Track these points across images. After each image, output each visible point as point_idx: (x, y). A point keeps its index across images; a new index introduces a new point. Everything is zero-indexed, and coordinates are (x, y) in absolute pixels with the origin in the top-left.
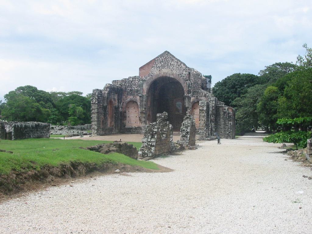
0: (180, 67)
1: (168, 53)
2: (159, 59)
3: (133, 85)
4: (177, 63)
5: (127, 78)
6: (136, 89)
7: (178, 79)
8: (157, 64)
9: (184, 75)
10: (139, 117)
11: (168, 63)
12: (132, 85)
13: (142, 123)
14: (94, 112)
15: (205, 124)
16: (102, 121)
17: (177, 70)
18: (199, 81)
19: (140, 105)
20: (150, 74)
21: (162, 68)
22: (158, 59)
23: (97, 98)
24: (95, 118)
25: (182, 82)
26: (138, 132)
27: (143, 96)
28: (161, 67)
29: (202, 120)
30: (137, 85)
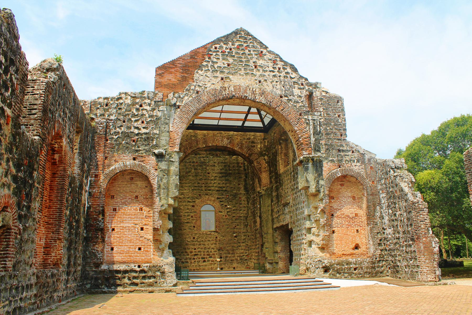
0: (283, 74)
1: (248, 34)
2: (221, 47)
4: (275, 62)
6: (143, 131)
8: (215, 60)
9: (296, 98)
11: (248, 61)
17: (274, 83)
18: (339, 116)
19: (159, 186)
20: (193, 87)
21: (229, 73)
22: (218, 46)
25: (292, 117)
28: (226, 71)
30: (149, 119)
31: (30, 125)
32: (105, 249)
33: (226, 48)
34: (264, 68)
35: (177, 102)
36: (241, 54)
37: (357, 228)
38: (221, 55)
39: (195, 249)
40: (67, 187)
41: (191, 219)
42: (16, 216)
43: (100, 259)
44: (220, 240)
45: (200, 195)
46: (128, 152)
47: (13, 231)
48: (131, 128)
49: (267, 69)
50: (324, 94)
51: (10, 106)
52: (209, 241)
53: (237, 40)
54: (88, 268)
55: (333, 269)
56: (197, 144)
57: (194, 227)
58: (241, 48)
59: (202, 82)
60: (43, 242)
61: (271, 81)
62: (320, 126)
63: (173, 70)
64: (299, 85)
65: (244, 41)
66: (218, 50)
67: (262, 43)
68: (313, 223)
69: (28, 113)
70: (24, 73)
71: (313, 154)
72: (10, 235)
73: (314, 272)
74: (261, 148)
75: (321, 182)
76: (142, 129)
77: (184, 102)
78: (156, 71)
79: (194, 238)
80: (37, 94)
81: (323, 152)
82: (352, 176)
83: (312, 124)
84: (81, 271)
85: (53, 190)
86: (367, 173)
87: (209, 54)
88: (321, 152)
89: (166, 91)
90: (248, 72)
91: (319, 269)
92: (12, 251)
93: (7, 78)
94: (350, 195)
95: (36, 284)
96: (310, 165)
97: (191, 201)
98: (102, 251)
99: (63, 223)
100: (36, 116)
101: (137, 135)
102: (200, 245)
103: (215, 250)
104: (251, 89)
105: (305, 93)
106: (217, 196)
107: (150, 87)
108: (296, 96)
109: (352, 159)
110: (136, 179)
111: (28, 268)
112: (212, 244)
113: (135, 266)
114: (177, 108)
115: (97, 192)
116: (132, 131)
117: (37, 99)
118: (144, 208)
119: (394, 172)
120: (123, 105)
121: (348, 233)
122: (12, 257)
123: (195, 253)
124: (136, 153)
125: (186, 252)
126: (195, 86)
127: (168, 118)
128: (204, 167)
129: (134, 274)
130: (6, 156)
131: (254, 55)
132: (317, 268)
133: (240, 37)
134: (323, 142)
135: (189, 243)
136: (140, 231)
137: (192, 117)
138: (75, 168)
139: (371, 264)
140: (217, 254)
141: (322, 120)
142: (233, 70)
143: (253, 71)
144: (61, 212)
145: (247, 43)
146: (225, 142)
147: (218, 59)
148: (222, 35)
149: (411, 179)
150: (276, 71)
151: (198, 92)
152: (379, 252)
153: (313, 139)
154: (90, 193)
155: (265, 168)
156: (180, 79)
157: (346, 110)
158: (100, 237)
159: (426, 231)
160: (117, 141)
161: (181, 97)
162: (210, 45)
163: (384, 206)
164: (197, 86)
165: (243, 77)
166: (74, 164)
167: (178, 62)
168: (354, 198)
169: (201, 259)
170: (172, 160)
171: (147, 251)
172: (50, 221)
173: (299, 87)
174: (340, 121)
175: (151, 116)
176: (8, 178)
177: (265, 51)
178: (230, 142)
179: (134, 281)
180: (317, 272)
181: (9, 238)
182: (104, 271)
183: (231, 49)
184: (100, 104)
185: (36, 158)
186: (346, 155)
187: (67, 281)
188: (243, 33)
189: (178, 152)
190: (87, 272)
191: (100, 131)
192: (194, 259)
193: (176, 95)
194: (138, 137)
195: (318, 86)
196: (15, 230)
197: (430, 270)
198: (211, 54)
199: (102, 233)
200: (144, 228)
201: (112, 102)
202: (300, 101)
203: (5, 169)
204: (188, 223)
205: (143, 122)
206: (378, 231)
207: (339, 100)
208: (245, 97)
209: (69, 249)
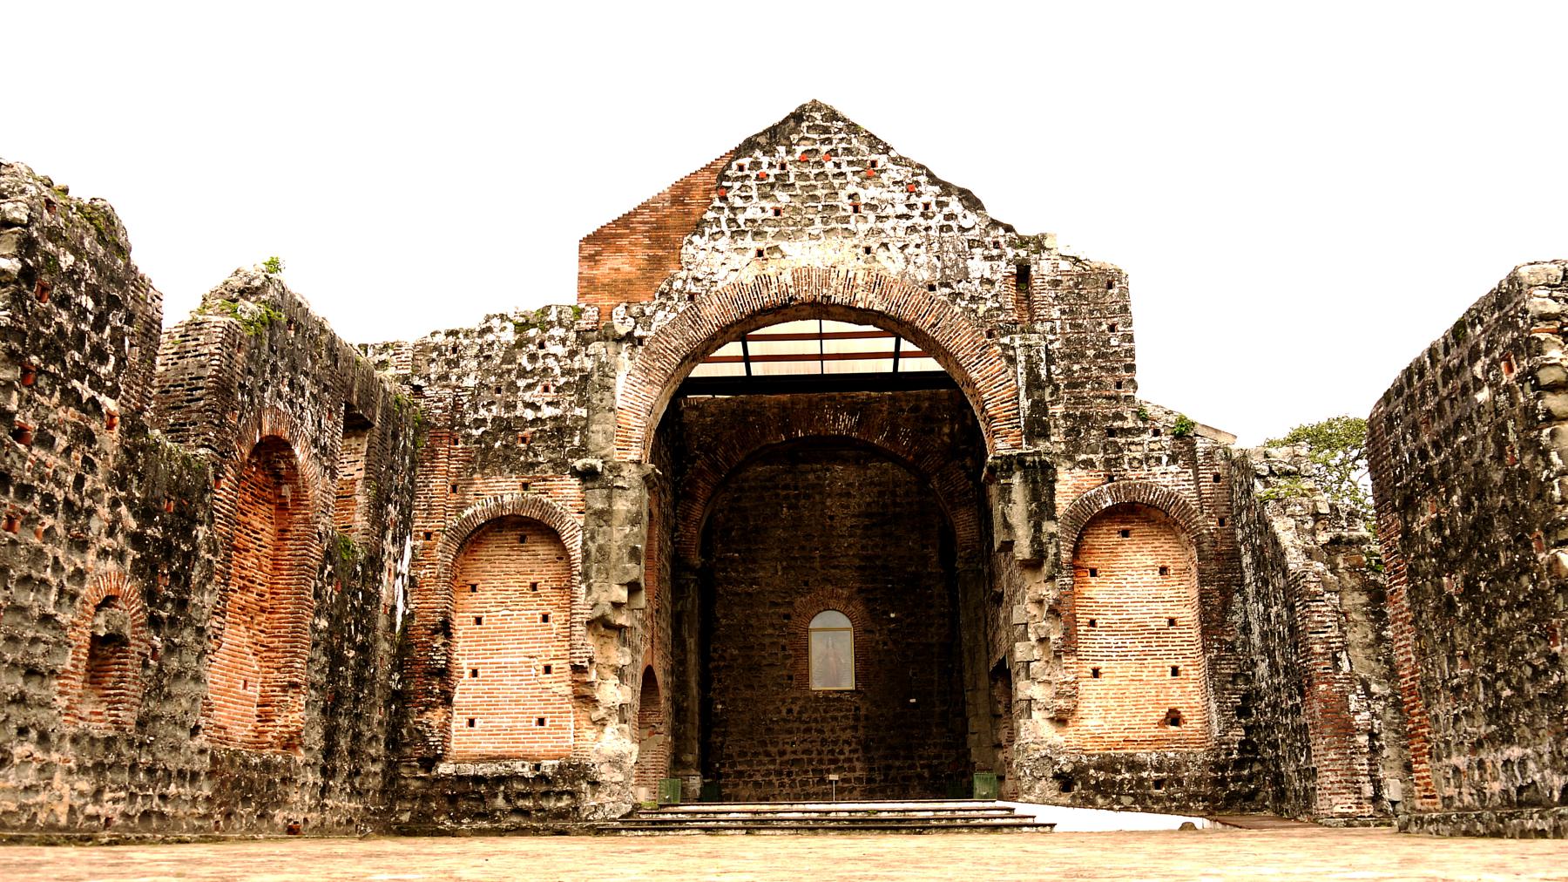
0: (939, 219)
1: (833, 116)
2: (756, 165)
3: (521, 383)
4: (912, 189)
5: (476, 323)
6: (547, 412)
8: (738, 203)
10: (577, 669)
12: (512, 387)
13: (602, 723)
16: (81, 638)
17: (911, 250)
18: (1112, 328)
20: (678, 285)
21: (776, 236)
22: (746, 161)
26: (561, 815)
27: (616, 469)
28: (770, 231)
30: (562, 381)
31: (191, 425)
32: (453, 725)
33: (771, 165)
34: (879, 210)
35: (635, 327)
36: (812, 176)
37: (1174, 663)
38: (755, 188)
40: (318, 563)
41: (780, 655)
42: (141, 618)
43: (436, 748)
44: (867, 718)
45: (806, 583)
46: (508, 470)
47: (132, 648)
48: (515, 407)
49: (889, 211)
50: (1065, 266)
51: (113, 393)
52: (835, 718)
54: (405, 772)
55: (1086, 785)
56: (763, 435)
58: (813, 160)
59: (704, 268)
60: (255, 692)
61: (901, 244)
62: (1050, 361)
63: (625, 242)
65: (823, 137)
66: (747, 172)
67: (875, 138)
68: (1033, 647)
69: (186, 398)
70: (149, 320)
71: (1025, 448)
72: (126, 657)
73: (1029, 788)
74: (951, 435)
76: (544, 407)
77: (653, 327)
79: (790, 711)
80: (205, 354)
81: (1057, 439)
82: (1149, 506)
83: (1022, 358)
84: (384, 777)
85: (279, 569)
86: (1200, 493)
88: (1052, 439)
89: (605, 301)
90: (834, 225)
91: (1043, 782)
92: (133, 690)
93: (101, 338)
94: (1150, 563)
95: (210, 775)
96: (1016, 480)
98: (445, 727)
99: (302, 648)
100: (202, 403)
101: (534, 422)
102: (808, 730)
103: (854, 746)
104: (843, 274)
105: (1004, 269)
106: (858, 585)
108: (977, 282)
109: (1155, 454)
110: (534, 538)
111: (183, 735)
112: (844, 730)
113: (523, 766)
114: (635, 346)
115: (428, 575)
116: (518, 413)
117: (203, 366)
118: (553, 614)
119: (1267, 484)
120: (495, 347)
121: (1144, 678)
122: (134, 704)
123: (794, 757)
124: (528, 470)
125: (768, 754)
126: (685, 281)
127: (612, 374)
128: (817, 497)
129: (519, 787)
130: (107, 496)
131: (850, 176)
132: (1040, 779)
133: (809, 127)
136: (541, 675)
137: (679, 366)
138: (358, 517)
139: (1211, 770)
140: (858, 759)
141: (1057, 345)
142: (789, 226)
143: (848, 222)
144: (299, 620)
145: (831, 143)
146: (845, 423)
147: (747, 198)
149: (1315, 506)
150: (916, 213)
151: (692, 297)
152: (1238, 734)
153: (1025, 403)
154: (411, 579)
155: (966, 494)
156: (643, 264)
157: (1131, 309)
158: (437, 691)
159: (1329, 664)
160: (480, 443)
161: (647, 313)
162: (726, 161)
163: (1251, 590)
164: (689, 281)
165: (819, 242)
166: (355, 508)
167: (639, 218)
168: (1163, 570)
170: (620, 483)
171: (560, 727)
172: (272, 642)
173: (986, 253)
174: (1114, 342)
175: (567, 372)
176: (115, 539)
177: (882, 160)
178: (859, 424)
179: (521, 803)
180: (1037, 791)
181: (125, 664)
182: (445, 778)
183: (783, 166)
184: (436, 348)
185: (202, 497)
186: (1133, 443)
187: (325, 790)
188: (817, 115)
189: (638, 463)
190: (403, 782)
191: (436, 419)
192: (789, 774)
193: (635, 310)
194: (533, 430)
195: (1047, 244)
196: (139, 646)
197: (1340, 782)
198: (731, 187)
199: (442, 680)
200: (554, 667)
201: (466, 342)
202: (989, 296)
203: (106, 520)
204: (771, 665)
205: (546, 389)
206: (1238, 671)
207: (1111, 279)
208: (825, 299)
209: (329, 712)
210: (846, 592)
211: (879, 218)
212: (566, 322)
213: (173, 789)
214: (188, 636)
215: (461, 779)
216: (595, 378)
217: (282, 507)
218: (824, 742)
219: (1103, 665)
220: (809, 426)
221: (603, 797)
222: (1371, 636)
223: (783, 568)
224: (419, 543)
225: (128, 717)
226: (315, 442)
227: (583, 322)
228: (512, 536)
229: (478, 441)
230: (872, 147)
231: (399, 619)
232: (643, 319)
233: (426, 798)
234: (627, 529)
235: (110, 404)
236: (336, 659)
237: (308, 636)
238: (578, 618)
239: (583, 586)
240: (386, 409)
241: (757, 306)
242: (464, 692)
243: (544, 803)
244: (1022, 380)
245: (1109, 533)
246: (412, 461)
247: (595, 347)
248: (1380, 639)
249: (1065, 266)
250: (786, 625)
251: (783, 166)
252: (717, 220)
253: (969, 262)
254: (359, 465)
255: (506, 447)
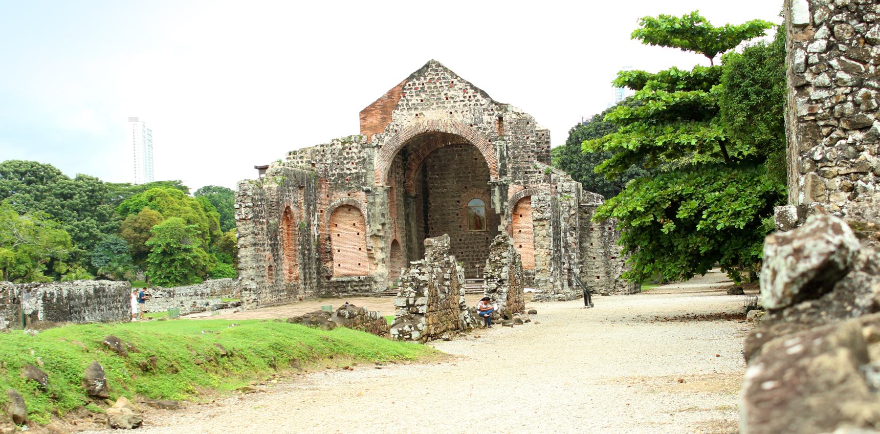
0: (473, 102)
1: (439, 65)
2: (414, 84)
3: (345, 162)
4: (465, 91)
5: (329, 142)
6: (354, 171)
7: (469, 138)
8: (409, 98)
9: (485, 125)
10: (368, 250)
12: (342, 163)
13: (377, 264)
14: (246, 243)
15: (549, 258)
16: (267, 268)
17: (465, 113)
18: (528, 138)
19: (369, 216)
20: (391, 127)
21: (422, 109)
22: (411, 83)
23: (251, 204)
24: (248, 259)
25: (480, 144)
26: (367, 291)
27: (376, 189)
28: (420, 107)
29: (542, 247)
30: (357, 161)
39: (462, 253)
45: (466, 188)
49: (458, 99)
52: (478, 242)
53: (430, 74)
54: (322, 280)
57: (460, 227)
60: (288, 267)
63: (374, 112)
64: (489, 111)
66: (411, 87)
75: (506, 204)
76: (353, 169)
78: (360, 115)
79: (461, 240)
87: (403, 93)
89: (369, 133)
90: (440, 105)
96: (497, 189)
97: (455, 195)
98: (332, 267)
102: (468, 247)
104: (443, 122)
105: (495, 118)
107: (356, 131)
108: (485, 123)
112: (482, 247)
123: (462, 258)
128: (470, 150)
131: (445, 87)
134: (510, 166)
135: (455, 246)
138: (303, 213)
144: (296, 249)
148: (415, 71)
150: (466, 100)
151: (396, 131)
153: (499, 165)
154: (318, 225)
156: (380, 120)
167: (378, 104)
169: (469, 265)
170: (377, 193)
171: (365, 266)
177: (455, 81)
179: (355, 288)
183: (423, 84)
184: (318, 151)
189: (382, 186)
193: (378, 136)
201: (327, 149)
204: (453, 222)
205: (353, 163)
209: (304, 269)
210: (482, 191)
211: (454, 102)
212: (357, 141)
213: (281, 294)
214: (279, 261)
215: (338, 282)
216: (367, 160)
217: (288, 220)
218: (474, 252)
219: (522, 244)
220: (453, 140)
221: (378, 286)
222: (600, 235)
223: (457, 181)
224: (319, 214)
225: (274, 281)
226: (294, 202)
227: (362, 141)
228: (346, 209)
229: (333, 181)
230: (452, 76)
231: (316, 237)
232: (380, 139)
233: (329, 288)
234: (380, 207)
235: (264, 220)
236: (304, 255)
237: (298, 252)
238: (367, 235)
239: (368, 226)
240: (307, 179)
241: (417, 134)
242: (336, 256)
243: (362, 288)
244: (498, 157)
245: (526, 203)
246: (315, 189)
247: (367, 150)
248: (602, 236)
249: (514, 116)
250: (458, 205)
251: (423, 84)
252: (402, 104)
253: (483, 116)
254: (303, 198)
255: (342, 182)
